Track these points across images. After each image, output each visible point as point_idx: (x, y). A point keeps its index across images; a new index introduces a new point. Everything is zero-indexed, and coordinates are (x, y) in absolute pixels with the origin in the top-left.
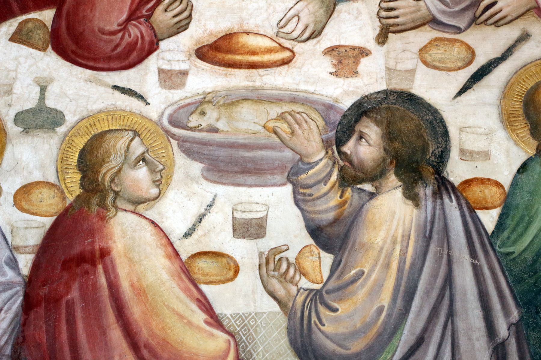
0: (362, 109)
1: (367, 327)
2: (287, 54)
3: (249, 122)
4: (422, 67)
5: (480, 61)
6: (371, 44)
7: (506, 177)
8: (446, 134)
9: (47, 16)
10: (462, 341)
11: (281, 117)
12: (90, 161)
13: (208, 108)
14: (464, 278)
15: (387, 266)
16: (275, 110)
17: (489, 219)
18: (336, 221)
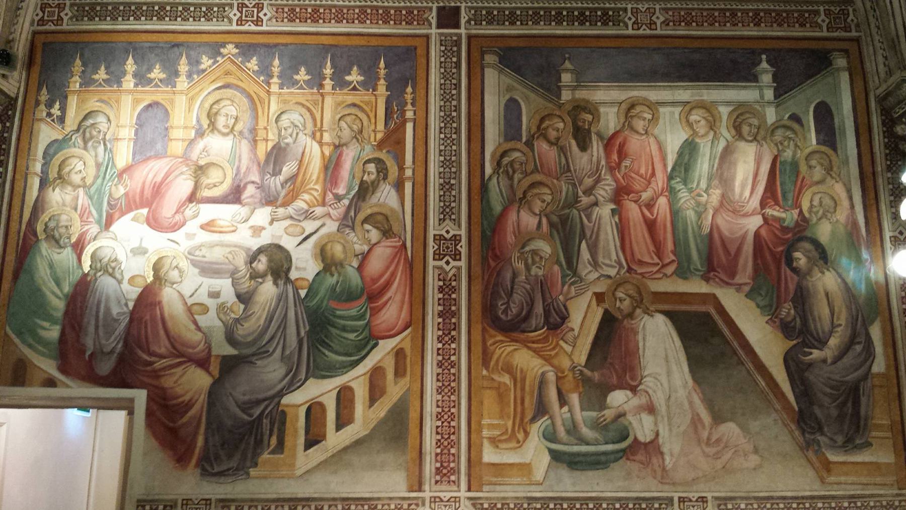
0: (260, 251)
1: (253, 333)
2: (233, 228)
3: (217, 255)
4: (285, 235)
5: (307, 233)
6: (267, 226)
7: (311, 278)
8: (291, 261)
9: (145, 211)
10: (288, 337)
11: (230, 253)
12: (157, 268)
13: (203, 248)
14: (291, 314)
15: (264, 309)
16: (228, 250)
17: (303, 293)
18: (247, 292)
